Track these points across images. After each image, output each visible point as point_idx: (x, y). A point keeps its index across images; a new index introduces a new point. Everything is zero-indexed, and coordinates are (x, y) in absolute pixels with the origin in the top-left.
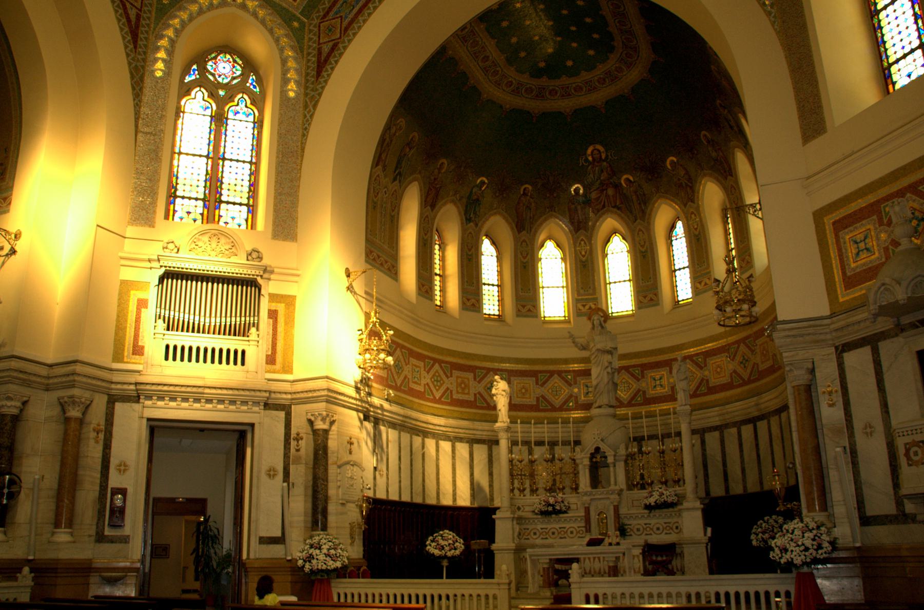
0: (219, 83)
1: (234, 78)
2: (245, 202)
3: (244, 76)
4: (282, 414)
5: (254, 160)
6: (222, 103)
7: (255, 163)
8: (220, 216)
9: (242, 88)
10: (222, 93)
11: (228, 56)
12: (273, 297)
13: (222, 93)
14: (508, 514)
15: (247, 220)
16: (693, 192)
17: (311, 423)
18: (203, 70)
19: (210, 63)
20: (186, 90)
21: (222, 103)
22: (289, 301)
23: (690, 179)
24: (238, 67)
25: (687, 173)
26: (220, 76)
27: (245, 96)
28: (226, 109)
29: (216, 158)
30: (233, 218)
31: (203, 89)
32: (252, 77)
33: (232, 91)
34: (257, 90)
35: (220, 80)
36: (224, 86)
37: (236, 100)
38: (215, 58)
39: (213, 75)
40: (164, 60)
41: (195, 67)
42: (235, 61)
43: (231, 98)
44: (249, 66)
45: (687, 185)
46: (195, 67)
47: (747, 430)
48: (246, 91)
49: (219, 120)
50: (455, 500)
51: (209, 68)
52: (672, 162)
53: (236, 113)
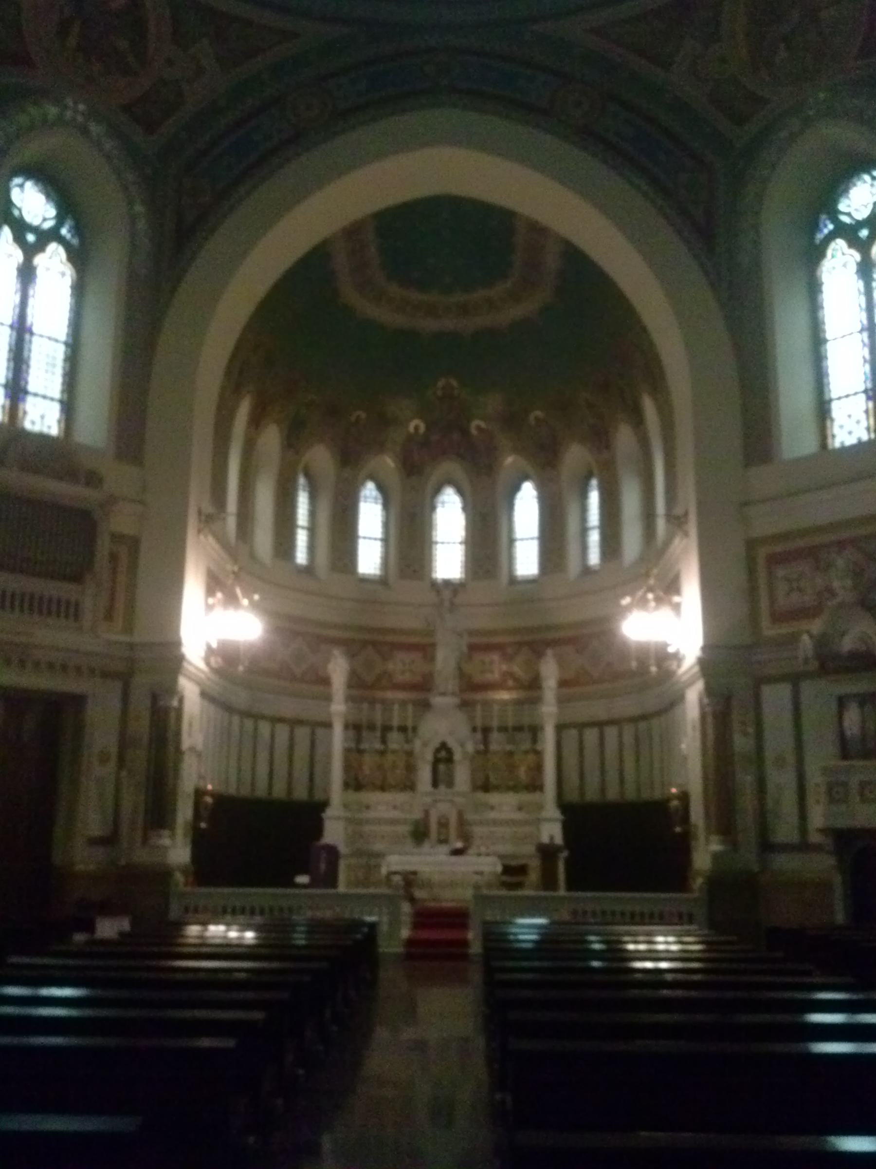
3: (60, 220)
4: (118, 685)
6: (30, 251)
10: (31, 238)
12: (117, 538)
14: (341, 813)
17: (155, 698)
21: (30, 251)
22: (134, 544)
33: (45, 237)
36: (35, 230)
47: (591, 736)
48: (61, 240)
50: (253, 790)
52: (537, 419)
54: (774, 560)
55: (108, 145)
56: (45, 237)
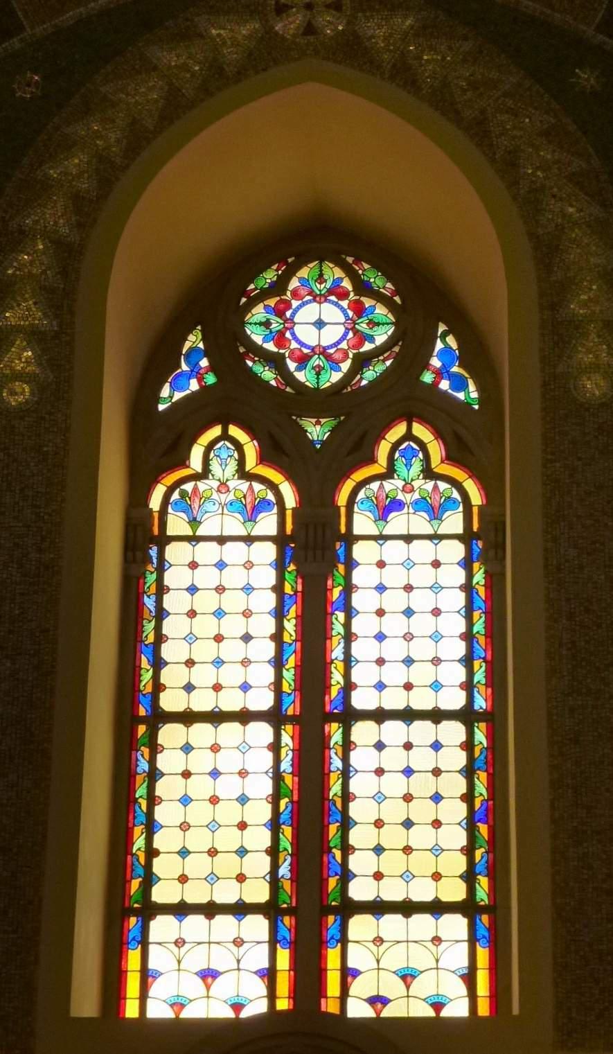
0: (300, 387)
1: (362, 362)
2: (455, 891)
3: (410, 346)
5: (480, 703)
7: (485, 716)
8: (348, 974)
9: (403, 396)
10: (317, 431)
11: (333, 273)
13: (317, 431)
15: (469, 979)
18: (229, 348)
19: (259, 313)
20: (160, 447)
24: (381, 311)
26: (303, 361)
27: (419, 430)
28: (342, 499)
29: (313, 712)
30: (407, 977)
31: (234, 431)
32: (445, 344)
33: (362, 415)
34: (471, 393)
35: (304, 377)
37: (383, 449)
38: (279, 287)
39: (276, 362)
40: (35, 336)
41: (194, 340)
42: (363, 288)
43: (354, 449)
44: (424, 298)
46: (194, 340)
49: (314, 555)
51: (257, 336)
53: (386, 509)
55: (429, 61)
56: (362, 415)
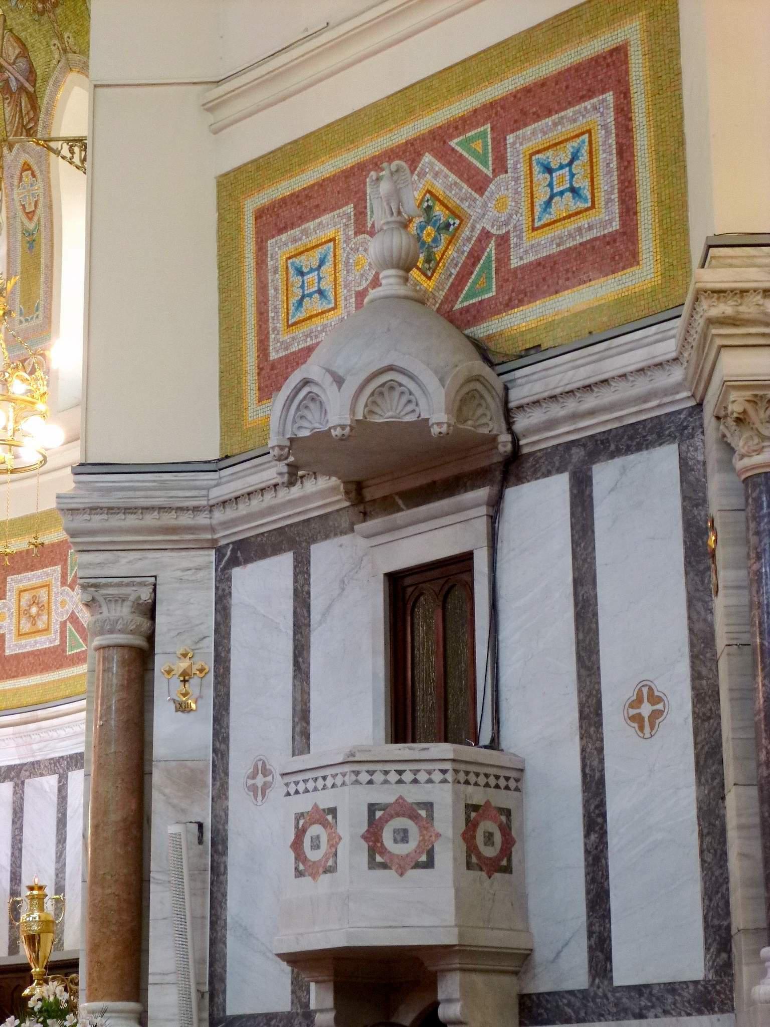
16: (34, 106)
23: (31, 74)
25: (24, 52)
45: (22, 88)
54: (276, 219)
